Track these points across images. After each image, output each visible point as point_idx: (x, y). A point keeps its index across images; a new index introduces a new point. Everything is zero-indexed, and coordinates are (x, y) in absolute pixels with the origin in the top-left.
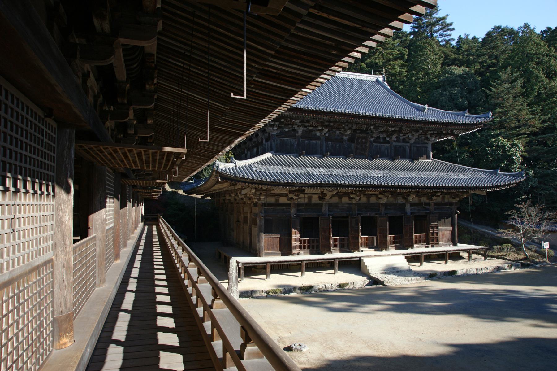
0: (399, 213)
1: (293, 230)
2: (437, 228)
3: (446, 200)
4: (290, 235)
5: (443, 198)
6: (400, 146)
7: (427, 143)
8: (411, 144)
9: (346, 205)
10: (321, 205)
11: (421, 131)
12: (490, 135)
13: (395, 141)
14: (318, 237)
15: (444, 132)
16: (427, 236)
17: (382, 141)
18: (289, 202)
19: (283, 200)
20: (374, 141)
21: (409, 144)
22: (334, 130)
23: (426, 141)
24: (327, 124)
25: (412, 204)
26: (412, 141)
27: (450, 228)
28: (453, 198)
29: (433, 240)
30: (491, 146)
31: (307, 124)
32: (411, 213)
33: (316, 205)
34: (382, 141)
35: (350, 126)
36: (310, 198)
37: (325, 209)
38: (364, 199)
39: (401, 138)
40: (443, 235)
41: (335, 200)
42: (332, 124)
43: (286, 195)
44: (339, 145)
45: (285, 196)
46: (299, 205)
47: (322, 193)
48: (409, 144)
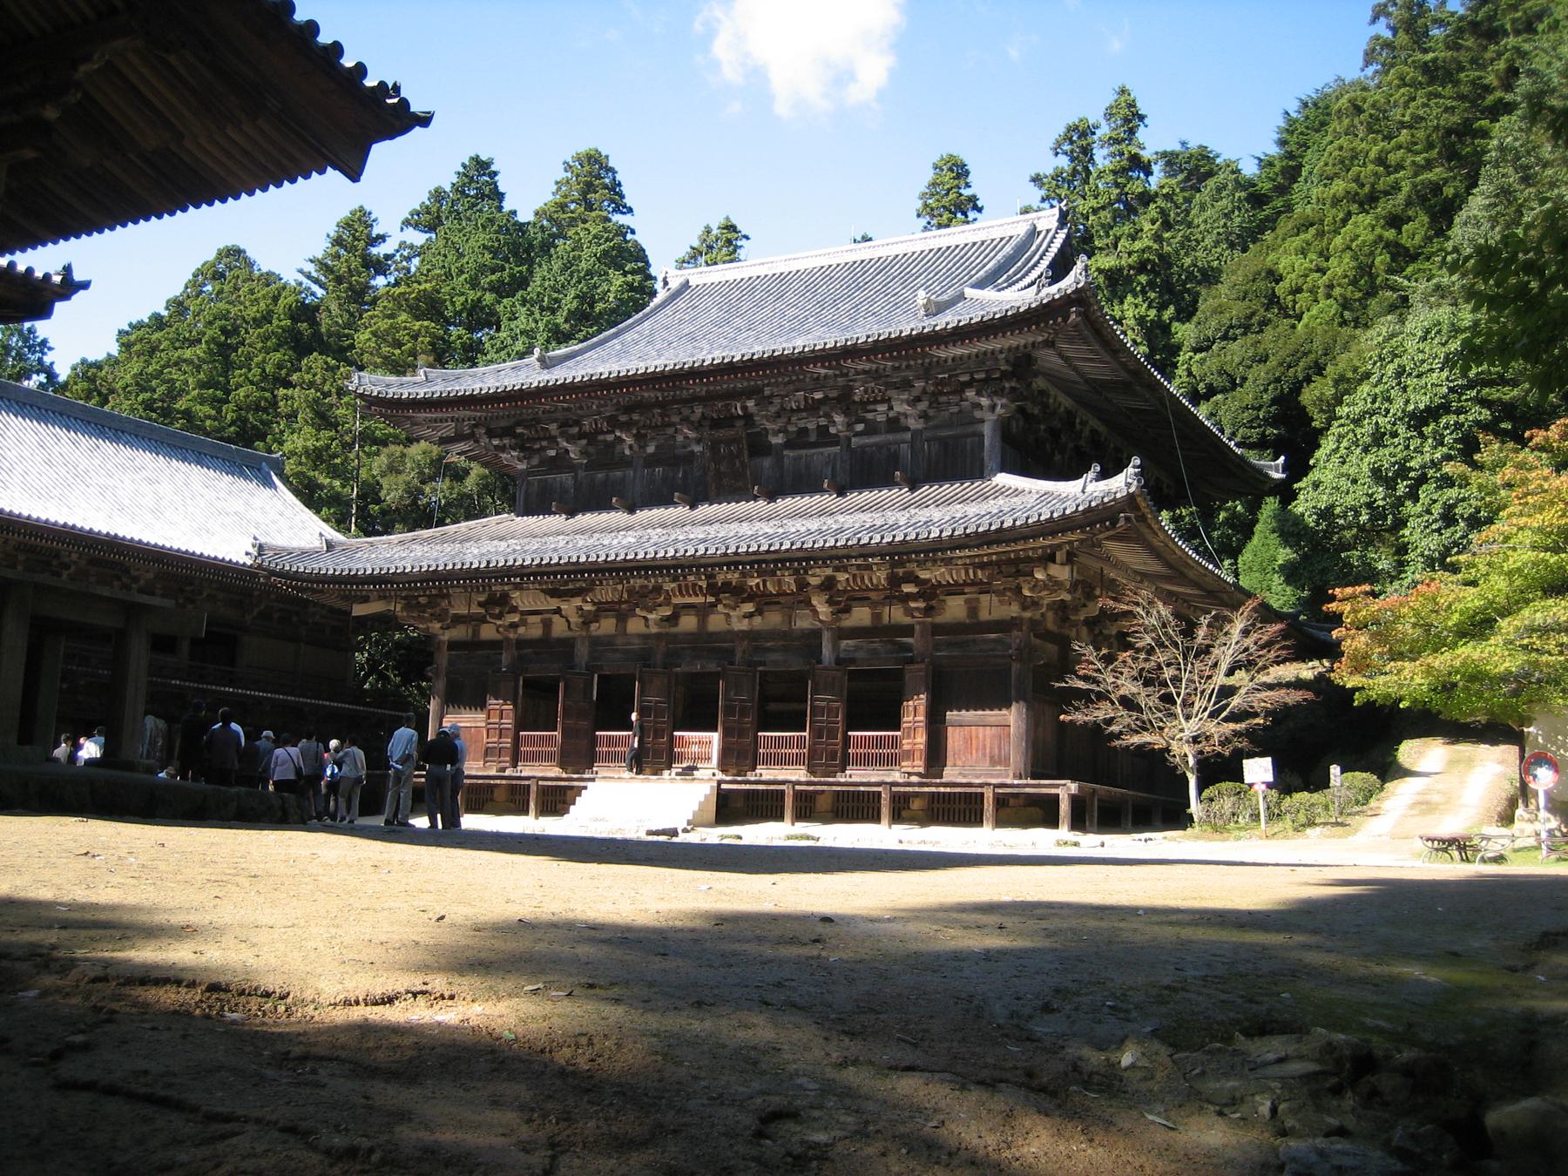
0: (796, 664)
3: (984, 615)
6: (879, 446)
8: (916, 433)
11: (919, 384)
17: (813, 438)
20: (789, 445)
21: (908, 436)
22: (671, 431)
24: (623, 418)
31: (575, 430)
34: (813, 438)
35: (686, 412)
36: (547, 625)
38: (688, 623)
40: (968, 740)
41: (607, 626)
42: (636, 417)
44: (685, 473)
48: (908, 436)
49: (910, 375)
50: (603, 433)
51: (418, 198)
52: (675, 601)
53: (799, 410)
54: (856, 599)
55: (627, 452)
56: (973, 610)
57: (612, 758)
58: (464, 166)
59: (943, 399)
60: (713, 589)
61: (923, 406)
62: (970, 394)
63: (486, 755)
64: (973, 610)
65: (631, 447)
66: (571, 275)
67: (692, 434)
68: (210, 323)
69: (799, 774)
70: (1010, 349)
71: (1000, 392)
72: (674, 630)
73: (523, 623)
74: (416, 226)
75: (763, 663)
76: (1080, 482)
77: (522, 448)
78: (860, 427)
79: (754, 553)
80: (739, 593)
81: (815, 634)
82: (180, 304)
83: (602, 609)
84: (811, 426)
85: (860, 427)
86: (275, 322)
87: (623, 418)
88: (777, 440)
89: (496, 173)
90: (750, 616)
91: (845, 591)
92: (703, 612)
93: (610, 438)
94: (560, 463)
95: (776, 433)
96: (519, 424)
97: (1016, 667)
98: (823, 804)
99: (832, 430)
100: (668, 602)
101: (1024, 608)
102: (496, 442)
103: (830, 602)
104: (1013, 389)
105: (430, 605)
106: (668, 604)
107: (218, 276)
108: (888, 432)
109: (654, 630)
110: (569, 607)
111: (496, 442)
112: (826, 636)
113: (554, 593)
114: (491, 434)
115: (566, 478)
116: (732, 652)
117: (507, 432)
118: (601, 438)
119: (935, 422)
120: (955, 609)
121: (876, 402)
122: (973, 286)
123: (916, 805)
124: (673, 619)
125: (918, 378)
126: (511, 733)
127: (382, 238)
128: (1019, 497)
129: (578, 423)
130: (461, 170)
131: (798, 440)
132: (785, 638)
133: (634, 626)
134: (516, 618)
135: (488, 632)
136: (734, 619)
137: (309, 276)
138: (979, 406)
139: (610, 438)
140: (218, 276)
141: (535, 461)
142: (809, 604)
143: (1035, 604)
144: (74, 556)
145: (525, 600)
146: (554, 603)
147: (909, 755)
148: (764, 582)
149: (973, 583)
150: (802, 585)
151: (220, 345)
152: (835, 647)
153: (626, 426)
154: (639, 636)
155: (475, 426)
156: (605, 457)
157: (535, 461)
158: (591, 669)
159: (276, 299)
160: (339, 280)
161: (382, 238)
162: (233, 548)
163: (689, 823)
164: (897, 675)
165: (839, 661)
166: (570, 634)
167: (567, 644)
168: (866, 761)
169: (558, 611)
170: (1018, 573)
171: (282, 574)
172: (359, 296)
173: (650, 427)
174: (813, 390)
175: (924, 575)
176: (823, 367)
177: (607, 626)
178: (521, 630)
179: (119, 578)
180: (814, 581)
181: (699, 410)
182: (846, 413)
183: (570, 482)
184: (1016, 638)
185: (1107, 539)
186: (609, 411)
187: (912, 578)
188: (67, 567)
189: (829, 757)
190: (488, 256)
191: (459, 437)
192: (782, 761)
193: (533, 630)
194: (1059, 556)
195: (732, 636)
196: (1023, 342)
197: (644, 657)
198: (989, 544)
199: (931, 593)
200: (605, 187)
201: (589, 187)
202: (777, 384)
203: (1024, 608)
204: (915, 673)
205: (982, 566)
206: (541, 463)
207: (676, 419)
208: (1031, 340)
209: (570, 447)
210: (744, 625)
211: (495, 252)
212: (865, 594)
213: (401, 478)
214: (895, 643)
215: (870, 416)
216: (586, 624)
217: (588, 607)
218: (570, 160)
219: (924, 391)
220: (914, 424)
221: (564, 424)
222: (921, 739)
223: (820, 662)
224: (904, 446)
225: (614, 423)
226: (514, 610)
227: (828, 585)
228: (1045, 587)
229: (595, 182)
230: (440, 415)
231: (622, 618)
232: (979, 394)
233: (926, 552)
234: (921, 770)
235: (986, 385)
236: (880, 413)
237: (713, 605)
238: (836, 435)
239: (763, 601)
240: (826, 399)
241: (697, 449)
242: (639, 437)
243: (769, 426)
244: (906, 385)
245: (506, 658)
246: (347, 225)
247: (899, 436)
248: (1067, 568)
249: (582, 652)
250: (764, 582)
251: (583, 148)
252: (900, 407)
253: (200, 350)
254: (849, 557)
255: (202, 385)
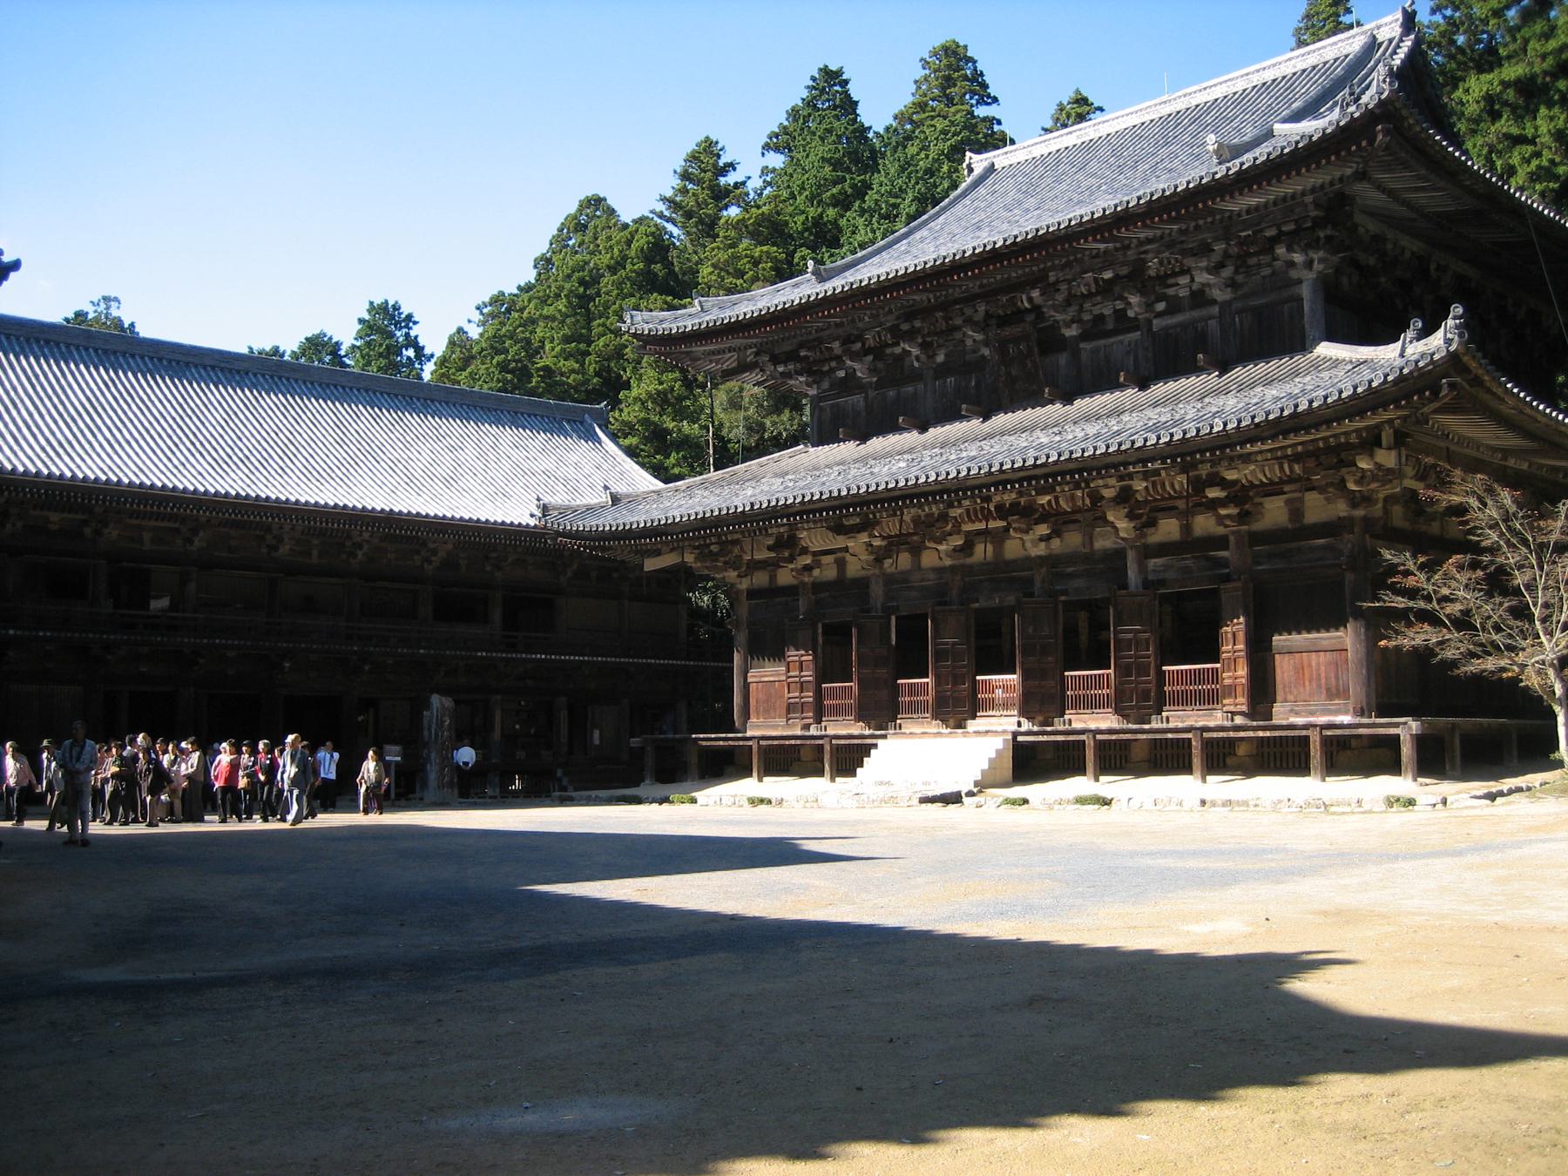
6: (1182, 325)
8: (1225, 305)
9: (932, 576)
17: (1110, 325)
20: (1085, 336)
21: (1215, 310)
22: (958, 335)
24: (905, 327)
25: (1148, 552)
31: (859, 345)
34: (1110, 325)
35: (968, 311)
36: (841, 564)
38: (983, 552)
40: (1299, 670)
42: (917, 324)
44: (978, 383)
48: (1215, 310)
49: (1207, 237)
50: (888, 346)
51: (777, 118)
52: (968, 527)
53: (1090, 295)
54: (1163, 509)
55: (916, 364)
56: (1296, 511)
57: (914, 708)
58: (813, 79)
59: (1252, 261)
60: (1002, 511)
61: (1227, 272)
62: (1281, 250)
63: (788, 712)
64: (1296, 511)
65: (917, 358)
66: (909, 178)
67: (979, 337)
68: (569, 276)
69: (1104, 721)
70: (1313, 190)
71: (1313, 244)
72: (969, 561)
73: (817, 564)
74: (777, 149)
75: (1065, 592)
76: (1399, 344)
77: (810, 372)
78: (1161, 306)
79: (1021, 469)
80: (1027, 514)
81: (1118, 555)
82: (549, 261)
83: (895, 544)
84: (1107, 312)
85: (1161, 306)
86: (629, 267)
87: (905, 327)
88: (1071, 332)
89: (846, 82)
90: (1046, 539)
91: (1146, 502)
92: (999, 537)
93: (897, 350)
94: (849, 384)
95: (1068, 325)
96: (801, 346)
97: (1349, 577)
98: (1138, 753)
99: (1131, 314)
100: (957, 530)
101: (1354, 505)
102: (781, 369)
103: (1131, 516)
104: (1329, 238)
105: (721, 553)
106: (959, 532)
107: (581, 228)
108: (1192, 308)
109: (948, 562)
110: (857, 544)
111: (781, 369)
112: (1131, 556)
113: (839, 529)
114: (775, 360)
115: (857, 400)
116: (1030, 581)
117: (791, 356)
118: (889, 351)
119: (1245, 289)
120: (1274, 512)
121: (1175, 274)
122: (1285, 121)
123: (1242, 750)
124: (967, 548)
125: (1217, 239)
126: (812, 687)
127: (731, 166)
128: (1341, 366)
129: (860, 338)
130: (811, 83)
131: (1096, 329)
132: (1089, 561)
133: (928, 559)
134: (808, 560)
135: (785, 577)
136: (1028, 544)
137: (661, 216)
138: (1292, 264)
139: (897, 350)
140: (581, 228)
141: (826, 385)
142: (1107, 522)
143: (1367, 500)
144: (366, 535)
145: (815, 539)
146: (840, 542)
147: (1231, 691)
148: (1057, 498)
149: (1291, 480)
150: (1096, 498)
151: (579, 297)
152: (1142, 568)
153: (910, 336)
154: (934, 569)
155: (757, 354)
156: (894, 372)
157: (826, 385)
158: (888, 611)
159: (629, 243)
160: (689, 215)
161: (731, 166)
162: (515, 510)
163: (976, 784)
164: (1214, 593)
165: (1147, 584)
166: (864, 573)
167: (862, 584)
168: (1184, 700)
169: (846, 549)
170: (1343, 463)
171: (565, 534)
172: (708, 228)
173: (936, 334)
174: (1103, 269)
175: (1231, 475)
176: (1095, 240)
177: (904, 560)
178: (816, 572)
179: (418, 552)
180: (1108, 493)
181: (982, 308)
182: (1142, 292)
183: (862, 403)
184: (1348, 542)
185: (1435, 411)
186: (890, 321)
187: (1216, 480)
188: (360, 547)
189: (1138, 698)
190: (828, 169)
191: (743, 368)
192: (1092, 704)
193: (828, 572)
194: (1387, 436)
195: (1029, 563)
196: (1328, 178)
197: (940, 594)
198: (1285, 433)
199: (1241, 495)
200: (966, 78)
201: (948, 82)
202: (1063, 267)
203: (1354, 505)
204: (1231, 592)
205: (1296, 458)
206: (831, 388)
207: (958, 321)
208: (1338, 174)
209: (856, 366)
210: (1040, 550)
211: (836, 165)
212: (1171, 503)
213: (742, 414)
214: (1208, 558)
215: (1171, 291)
216: (879, 561)
217: (877, 543)
218: (926, 56)
219: (1226, 255)
220: (1219, 295)
221: (847, 341)
222: (1242, 671)
223: (1125, 586)
224: (1213, 323)
225: (898, 335)
226: (805, 551)
227: (1125, 496)
228: (1374, 478)
229: (955, 75)
230: (712, 348)
231: (916, 551)
232: (1290, 249)
233: (1212, 450)
234: (1244, 708)
235: (1299, 237)
236: (1182, 287)
237: (1006, 529)
238: (1136, 319)
239: (1059, 521)
240: (1117, 277)
241: (986, 352)
242: (925, 346)
243: (1059, 317)
244: (1205, 249)
245: (802, 605)
246: (693, 158)
247: (1203, 312)
248: (1394, 453)
249: (877, 591)
250: (1057, 498)
251: (938, 42)
252: (1202, 278)
253: (561, 305)
254: (1126, 464)
255: (567, 340)
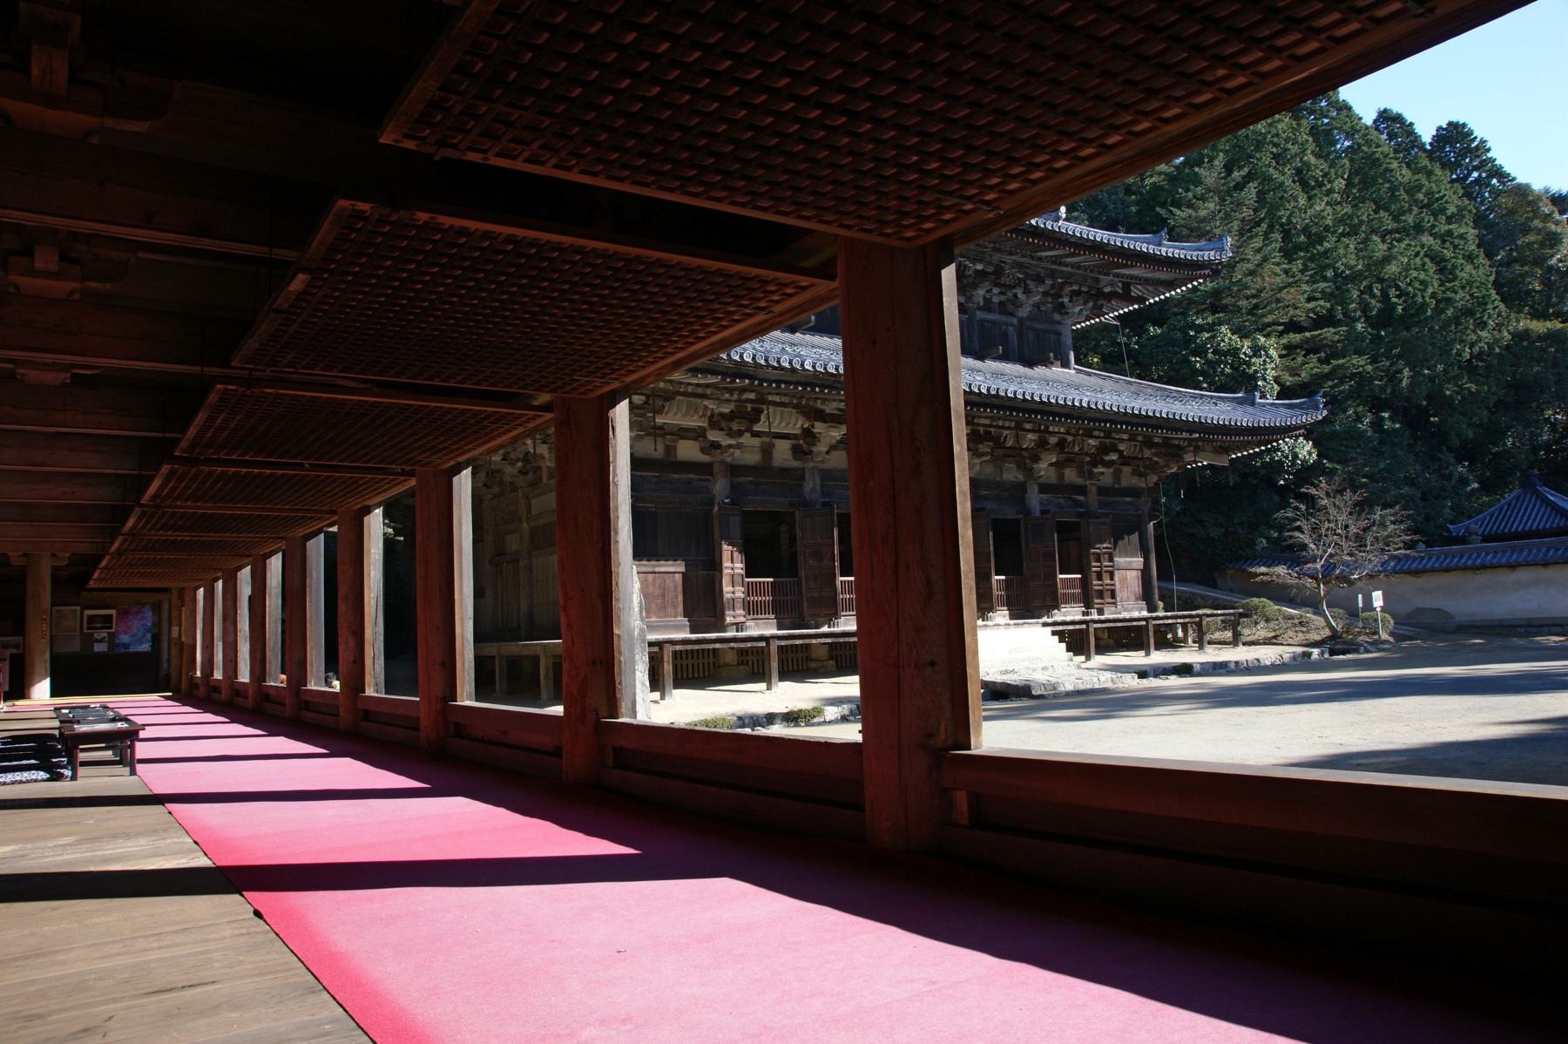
0: (1010, 514)
1: (727, 549)
2: (1111, 560)
4: (715, 566)
5: (1117, 476)
6: (993, 323)
7: (1059, 323)
8: (1021, 320)
10: (799, 475)
12: (1193, 326)
13: (979, 308)
14: (796, 575)
15: (1107, 290)
16: (1085, 583)
18: (705, 458)
19: (688, 450)
21: (1015, 321)
23: (1057, 317)
25: (1044, 488)
26: (1024, 312)
27: (1138, 561)
28: (1140, 476)
29: (1100, 594)
30: (1200, 351)
32: (1043, 512)
33: (785, 471)
36: (767, 451)
37: (811, 485)
39: (995, 300)
43: (698, 434)
45: (695, 439)
46: (735, 470)
47: (808, 433)
56: (1117, 476)
